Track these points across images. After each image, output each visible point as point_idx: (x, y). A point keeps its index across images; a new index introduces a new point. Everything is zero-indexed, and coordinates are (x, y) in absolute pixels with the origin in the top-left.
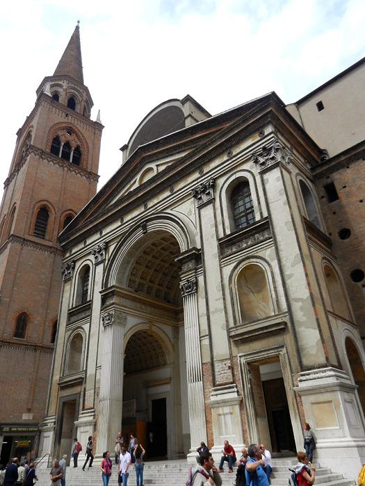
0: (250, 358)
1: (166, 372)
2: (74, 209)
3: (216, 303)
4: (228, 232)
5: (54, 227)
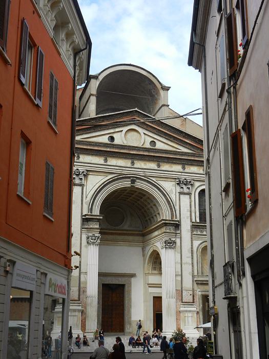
0: (204, 293)
3: (187, 259)
4: (198, 221)
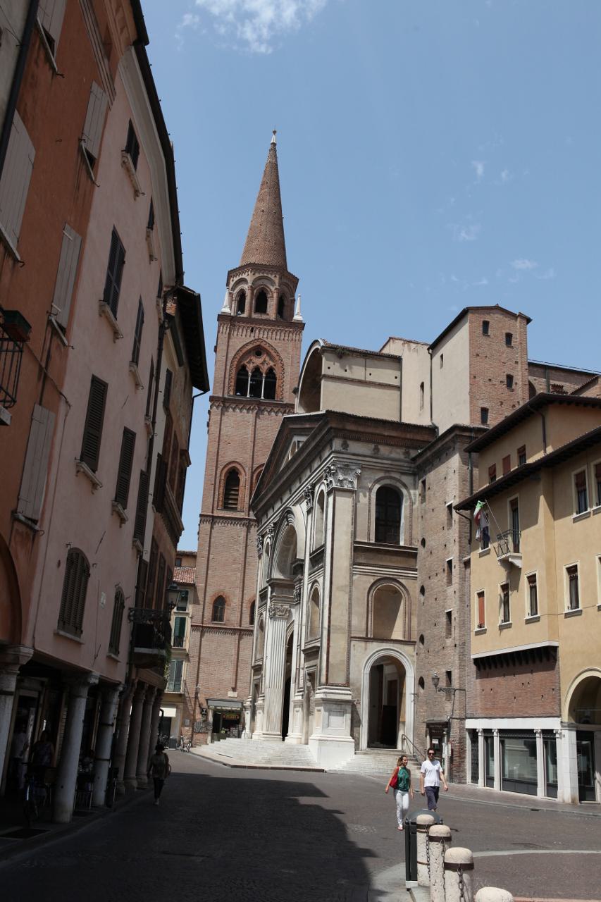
5: (244, 494)
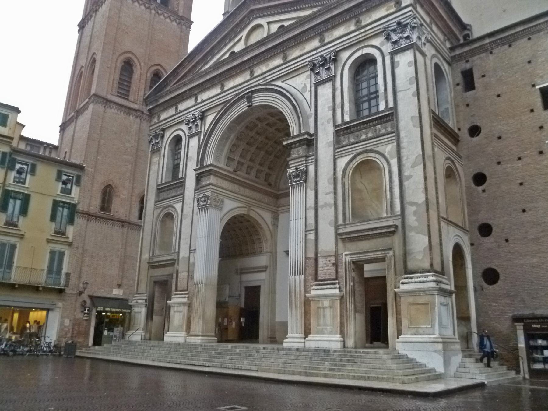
0: (356, 258)
1: (262, 260)
2: (162, 64)
3: (326, 198)
4: (347, 119)
